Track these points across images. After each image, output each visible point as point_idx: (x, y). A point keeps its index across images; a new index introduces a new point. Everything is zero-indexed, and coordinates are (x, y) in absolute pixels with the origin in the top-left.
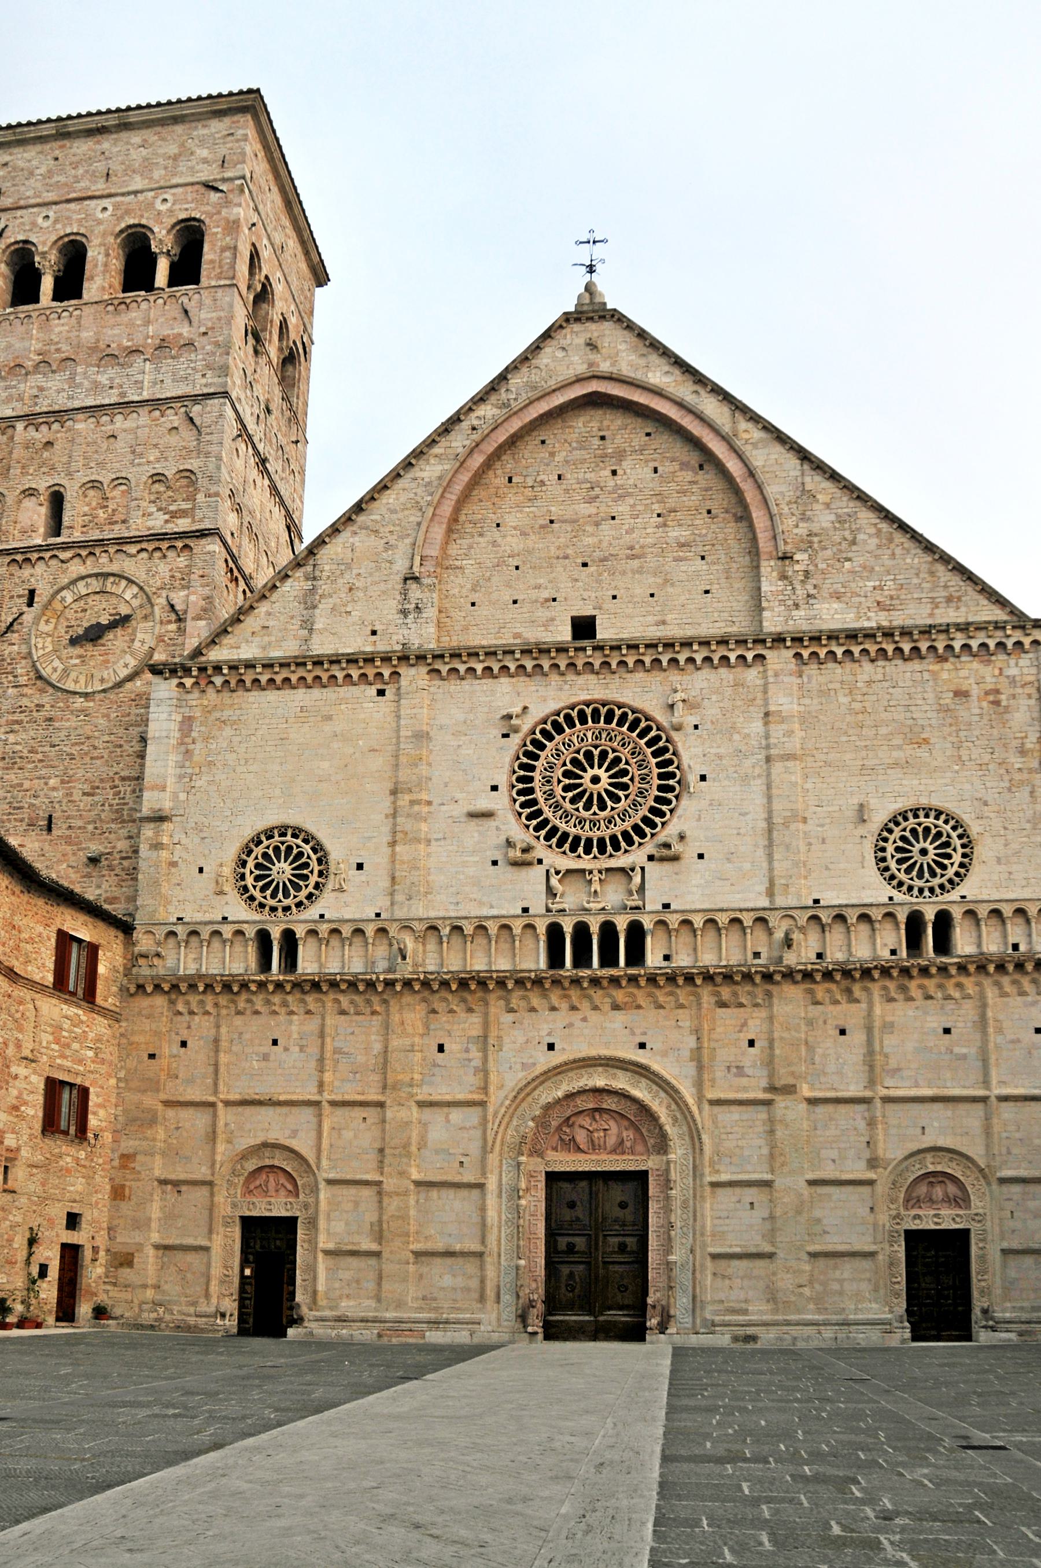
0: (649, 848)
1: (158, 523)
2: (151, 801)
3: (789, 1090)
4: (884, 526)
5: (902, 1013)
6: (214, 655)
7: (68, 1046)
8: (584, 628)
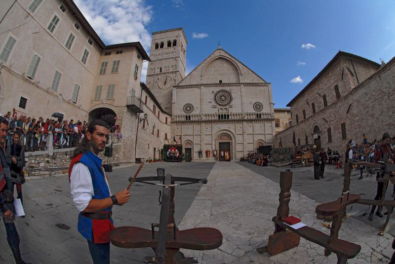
1: (172, 70)
6: (180, 85)
8: (221, 81)
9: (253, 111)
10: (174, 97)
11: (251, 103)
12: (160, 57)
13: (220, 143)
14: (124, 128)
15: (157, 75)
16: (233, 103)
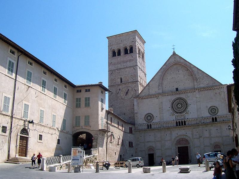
0: (185, 113)
2: (135, 111)
3: (201, 137)
4: (207, 75)
5: (212, 128)
7: (130, 138)
8: (177, 89)
9: (208, 115)
10: (136, 107)
11: (207, 107)
12: (119, 66)
13: (178, 148)
14: (99, 144)
15: (119, 85)
16: (189, 109)
